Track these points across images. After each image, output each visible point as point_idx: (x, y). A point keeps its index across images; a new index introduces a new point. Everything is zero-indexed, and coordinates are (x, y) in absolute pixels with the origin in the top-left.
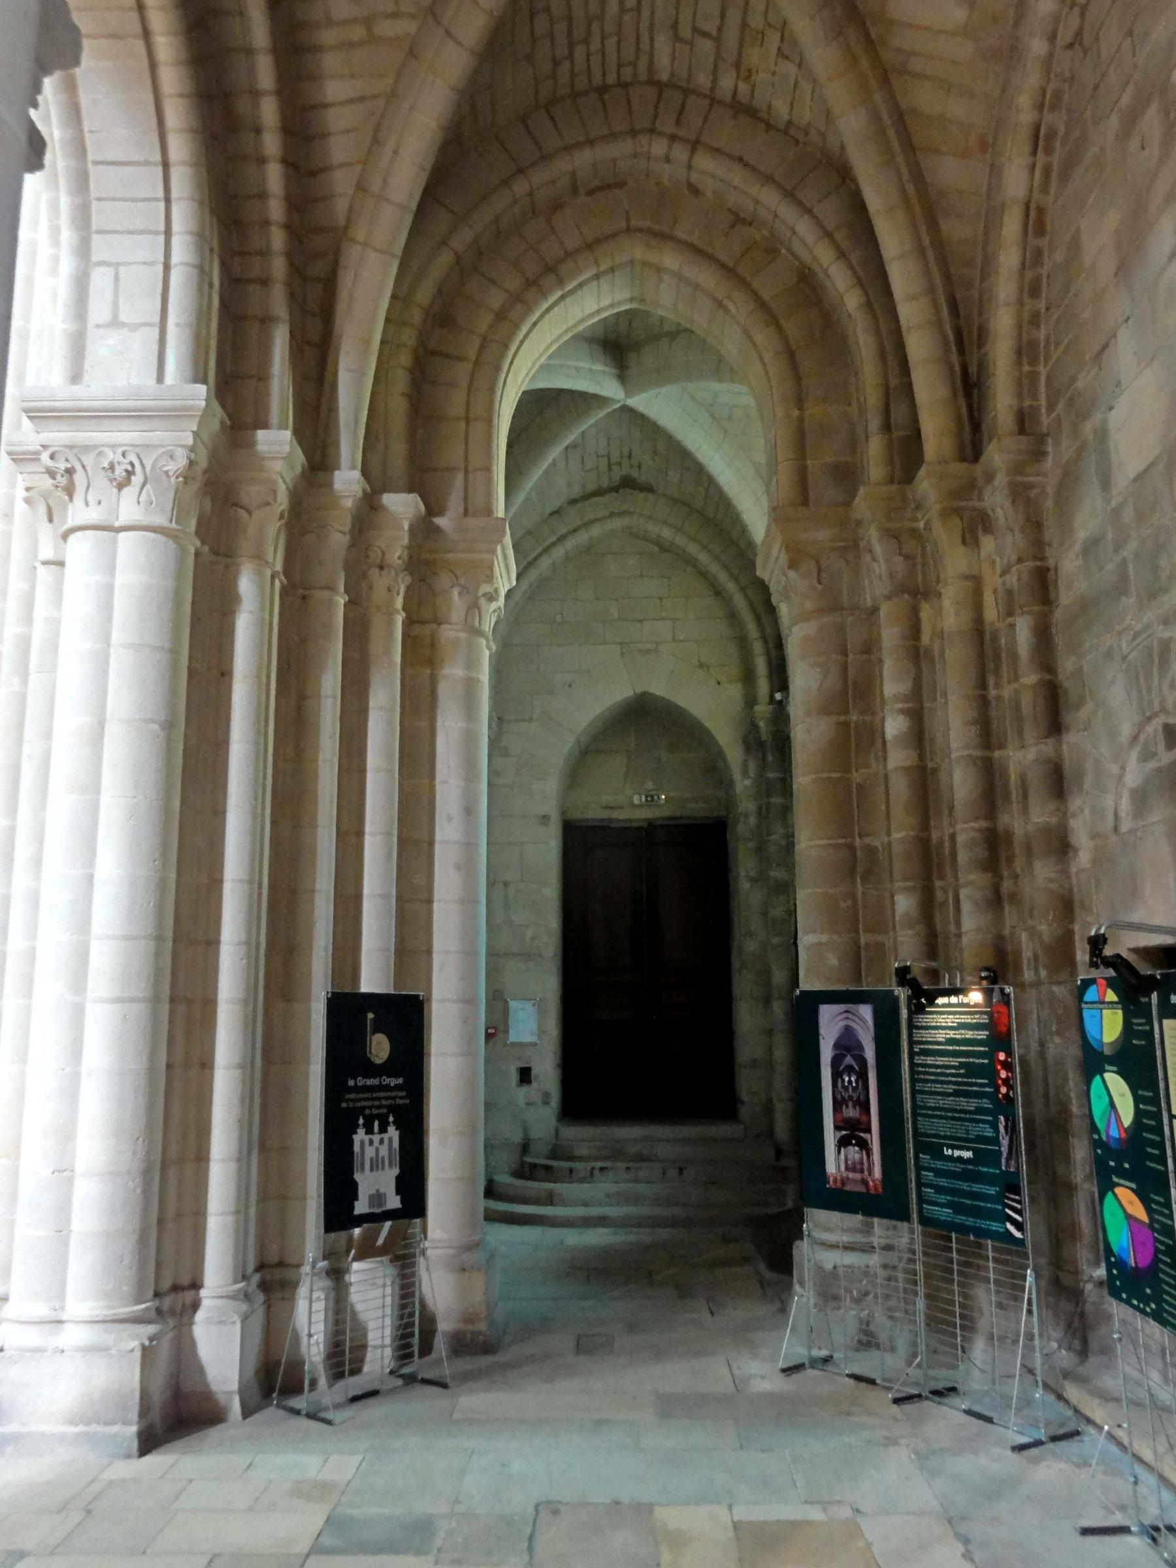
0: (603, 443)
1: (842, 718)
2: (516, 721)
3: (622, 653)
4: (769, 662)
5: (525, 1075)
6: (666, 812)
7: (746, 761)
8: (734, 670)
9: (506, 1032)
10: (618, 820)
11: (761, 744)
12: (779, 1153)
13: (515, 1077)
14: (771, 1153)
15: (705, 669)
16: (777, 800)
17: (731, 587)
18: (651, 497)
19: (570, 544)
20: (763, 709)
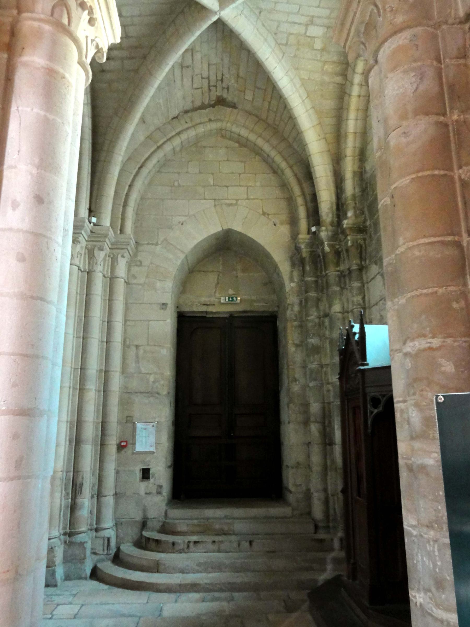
0: (205, 66)
1: (442, 119)
2: (148, 244)
3: (215, 206)
4: (308, 211)
5: (146, 474)
6: (239, 308)
7: (292, 271)
8: (284, 217)
9: (134, 444)
10: (212, 313)
11: (302, 261)
12: (316, 527)
13: (139, 475)
14: (311, 528)
15: (266, 216)
16: (312, 294)
17: (283, 165)
18: (235, 111)
19: (184, 136)
20: (303, 237)
